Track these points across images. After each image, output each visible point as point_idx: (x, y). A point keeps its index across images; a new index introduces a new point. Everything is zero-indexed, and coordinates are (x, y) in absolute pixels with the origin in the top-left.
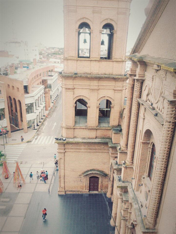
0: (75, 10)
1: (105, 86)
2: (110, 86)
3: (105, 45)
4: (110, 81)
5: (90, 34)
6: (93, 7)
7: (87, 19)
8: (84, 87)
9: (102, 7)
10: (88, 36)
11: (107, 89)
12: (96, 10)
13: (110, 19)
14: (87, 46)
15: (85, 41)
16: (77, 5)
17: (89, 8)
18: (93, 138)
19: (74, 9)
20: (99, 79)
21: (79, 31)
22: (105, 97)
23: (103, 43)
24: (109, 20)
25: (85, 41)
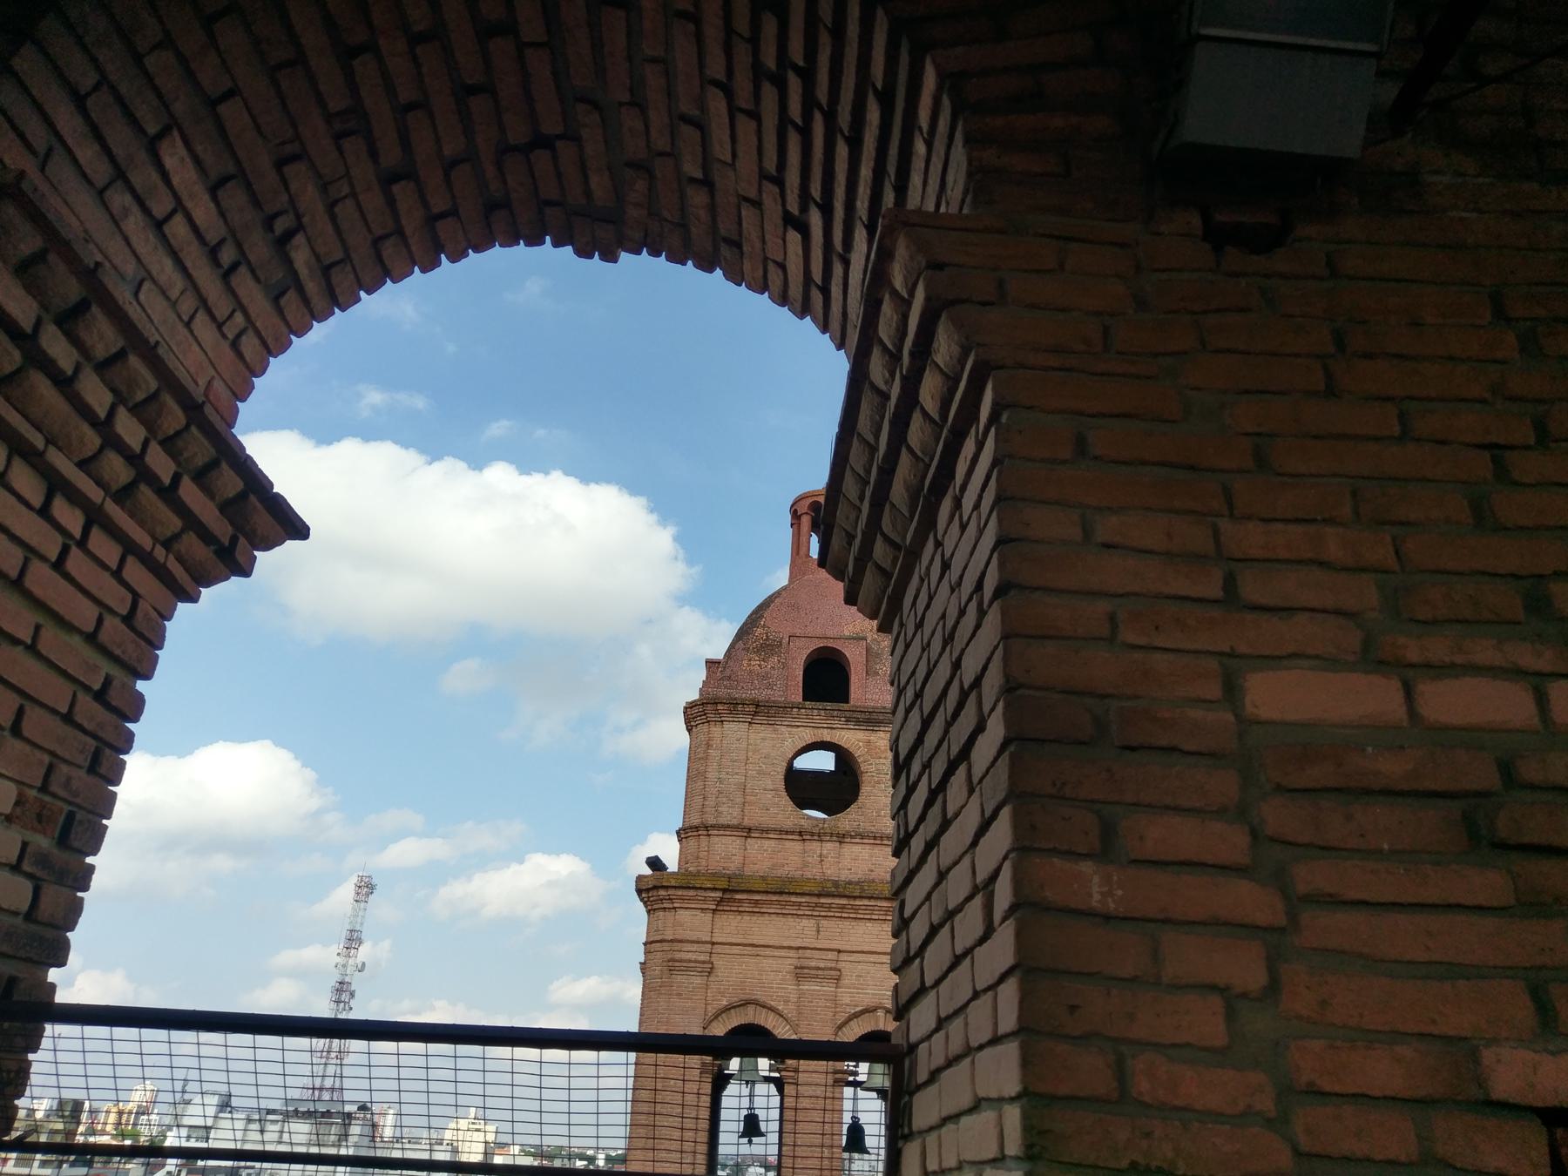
0: (704, 962)
5: (779, 1084)
6: (798, 948)
7: (764, 1007)
9: (839, 951)
10: (767, 1102)
12: (813, 964)
14: (767, 1146)
15: (751, 1127)
16: (714, 940)
17: (777, 953)
19: (702, 958)
21: (721, 1069)
23: (856, 1133)
24: (880, 1013)
25: (751, 1127)
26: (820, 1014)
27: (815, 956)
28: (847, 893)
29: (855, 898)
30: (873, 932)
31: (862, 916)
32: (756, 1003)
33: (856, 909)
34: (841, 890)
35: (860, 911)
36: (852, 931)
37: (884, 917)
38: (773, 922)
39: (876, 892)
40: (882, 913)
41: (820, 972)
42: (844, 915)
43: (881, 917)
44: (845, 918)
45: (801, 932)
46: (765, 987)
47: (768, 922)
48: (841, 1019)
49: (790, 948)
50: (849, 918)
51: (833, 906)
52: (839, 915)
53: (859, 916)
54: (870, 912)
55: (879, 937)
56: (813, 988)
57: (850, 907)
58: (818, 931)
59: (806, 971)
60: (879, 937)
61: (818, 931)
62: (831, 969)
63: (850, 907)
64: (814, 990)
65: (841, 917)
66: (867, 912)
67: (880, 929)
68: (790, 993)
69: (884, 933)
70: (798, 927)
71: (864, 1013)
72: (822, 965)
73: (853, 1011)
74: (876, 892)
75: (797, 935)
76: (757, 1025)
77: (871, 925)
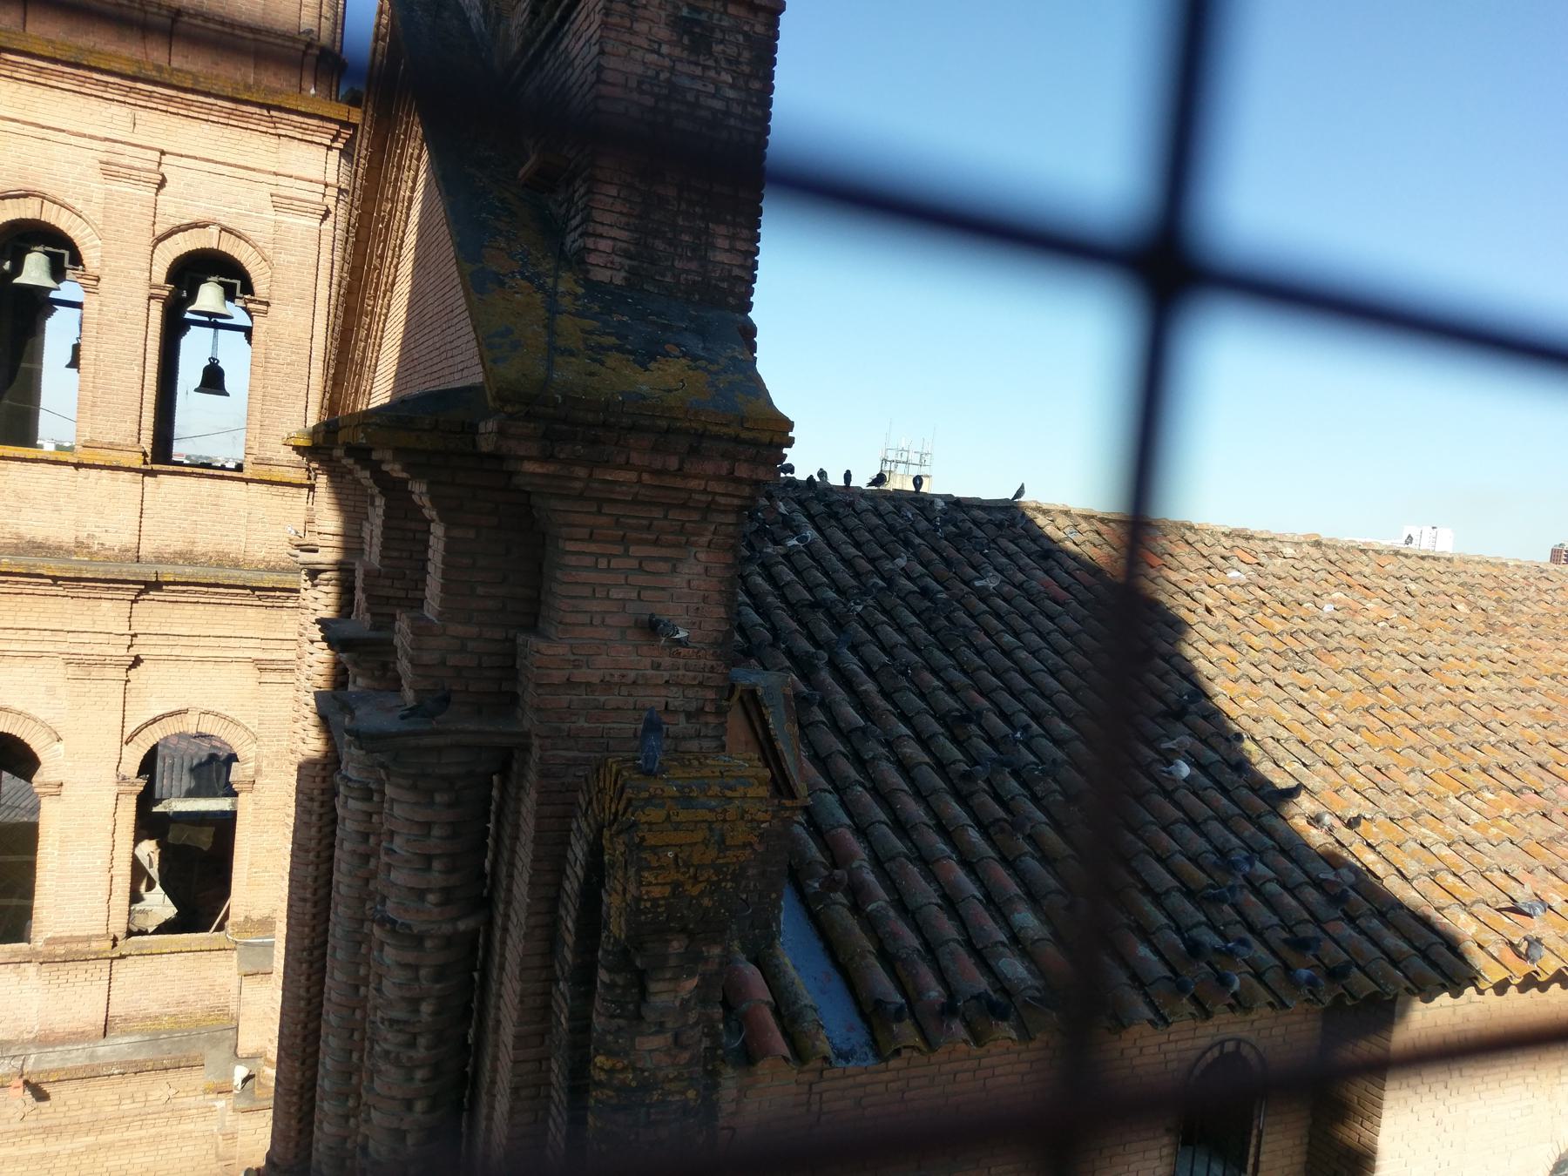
1: (184, 641)
2: (223, 643)
3: (228, 395)
4: (222, 608)
8: (15, 646)
11: (202, 660)
13: (224, 229)
18: (78, 1037)
20: (141, 592)
22: (179, 712)
24: (214, 230)
26: (133, 221)
27: (126, 152)
28: (175, 82)
29: (185, 90)
30: (210, 137)
31: (196, 115)
32: (44, 197)
33: (188, 105)
34: (166, 76)
35: (192, 108)
36: (180, 130)
37: (226, 121)
38: (67, 101)
39: (216, 87)
40: (223, 115)
41: (134, 172)
42: (170, 109)
43: (222, 120)
44: (171, 113)
45: (110, 120)
46: (56, 179)
47: (60, 100)
48: (161, 229)
49: (92, 137)
50: (178, 114)
51: (155, 95)
52: (164, 108)
53: (191, 114)
54: (206, 111)
55: (218, 143)
56: (123, 189)
57: (179, 100)
58: (135, 124)
59: (114, 168)
60: (218, 143)
61: (135, 124)
62: (149, 171)
63: (179, 100)
64: (126, 193)
65: (167, 112)
66: (203, 110)
67: (221, 134)
68: (93, 191)
69: (224, 139)
70: (104, 114)
71: (192, 228)
72: (138, 164)
73: (178, 224)
74: (216, 87)
75: (103, 124)
76: (45, 222)
77: (207, 127)
